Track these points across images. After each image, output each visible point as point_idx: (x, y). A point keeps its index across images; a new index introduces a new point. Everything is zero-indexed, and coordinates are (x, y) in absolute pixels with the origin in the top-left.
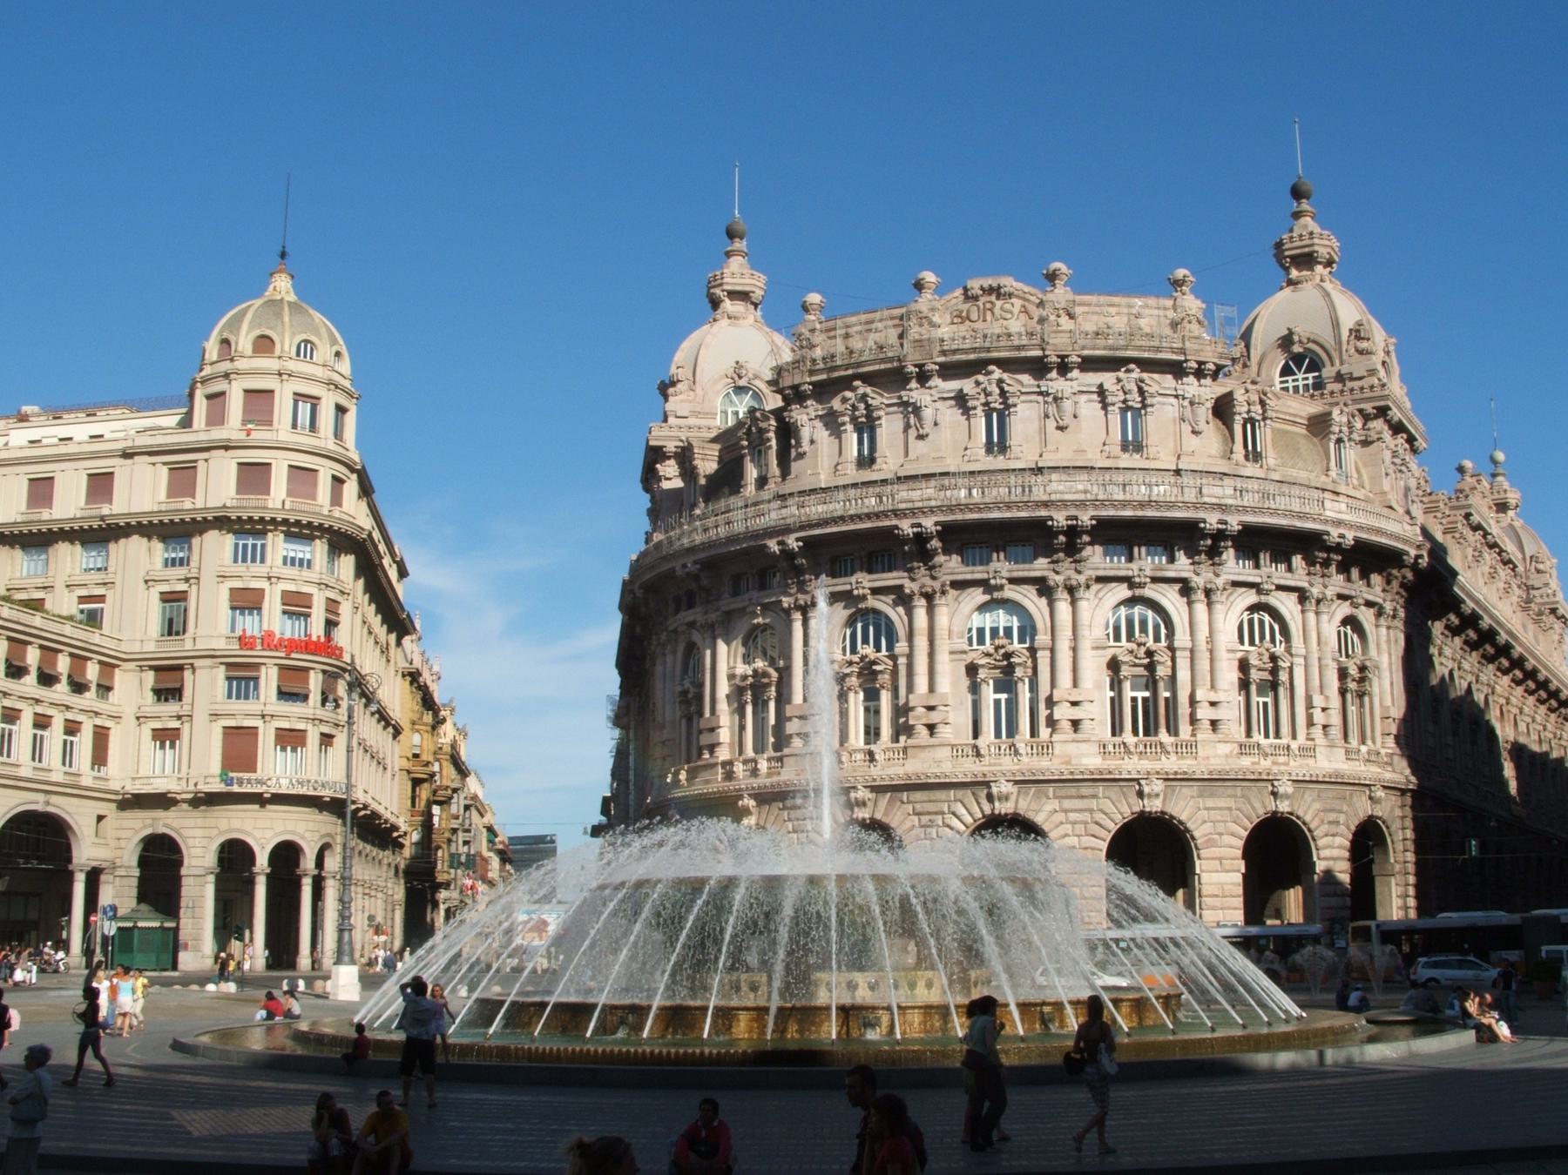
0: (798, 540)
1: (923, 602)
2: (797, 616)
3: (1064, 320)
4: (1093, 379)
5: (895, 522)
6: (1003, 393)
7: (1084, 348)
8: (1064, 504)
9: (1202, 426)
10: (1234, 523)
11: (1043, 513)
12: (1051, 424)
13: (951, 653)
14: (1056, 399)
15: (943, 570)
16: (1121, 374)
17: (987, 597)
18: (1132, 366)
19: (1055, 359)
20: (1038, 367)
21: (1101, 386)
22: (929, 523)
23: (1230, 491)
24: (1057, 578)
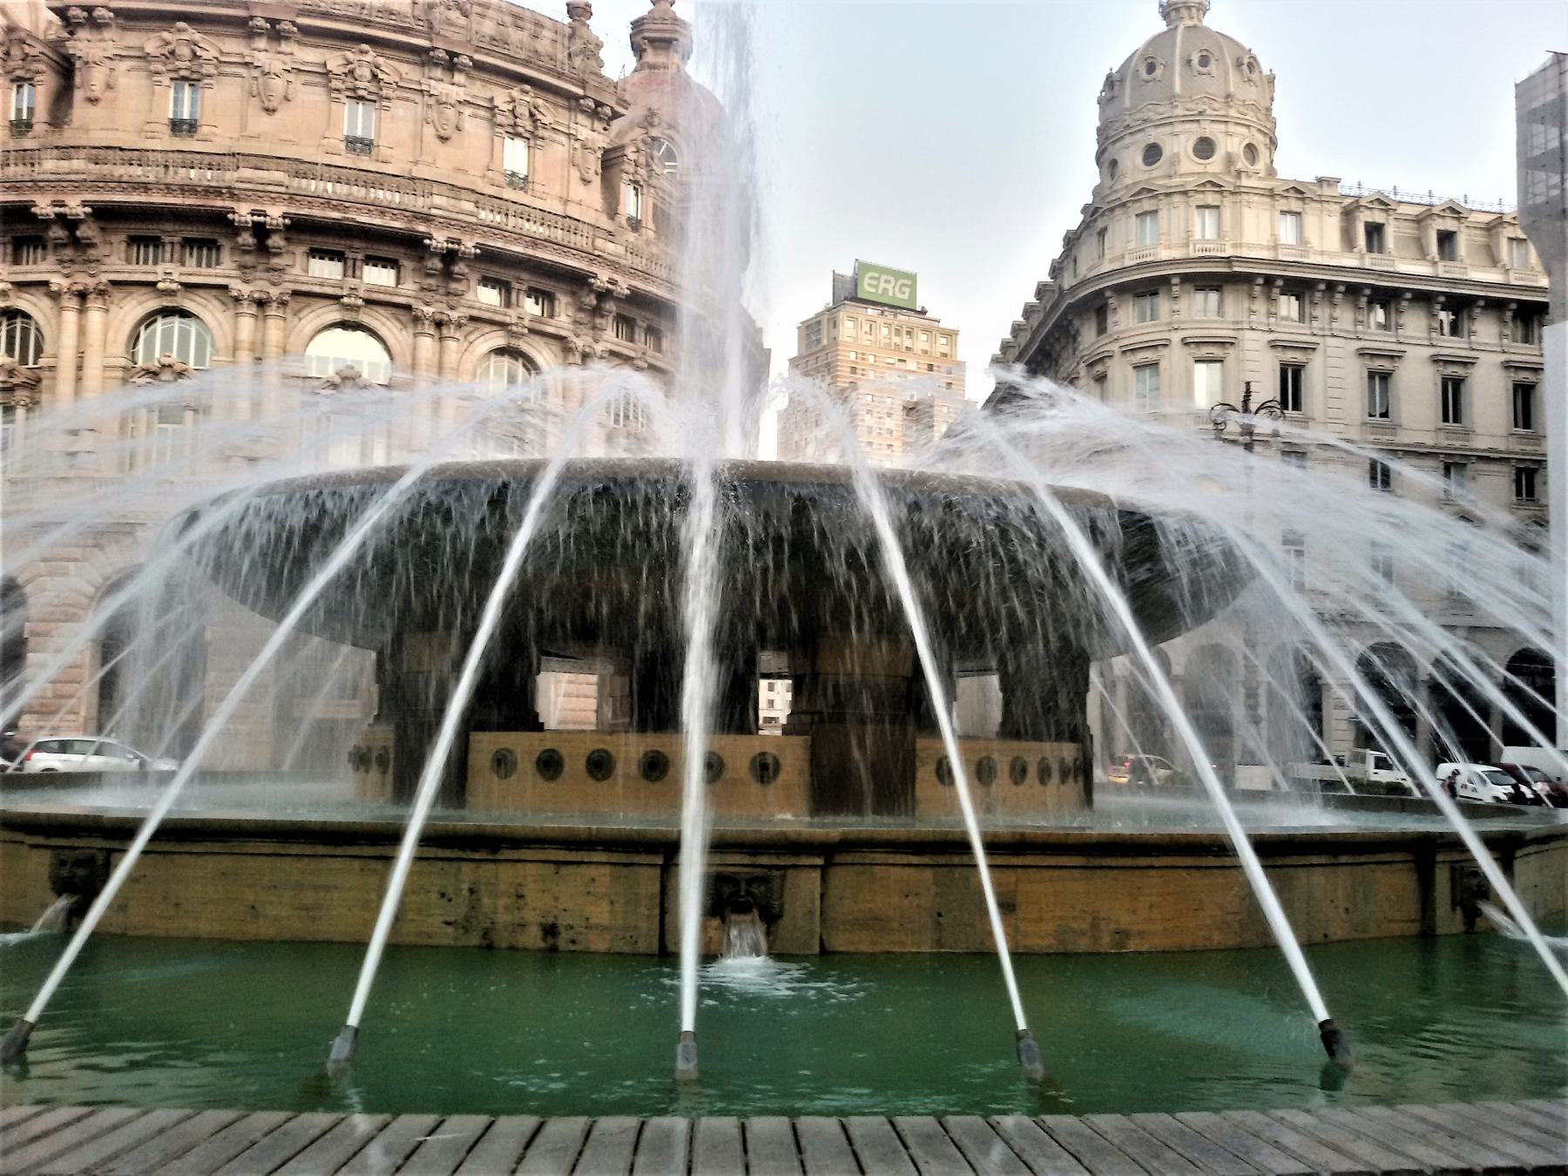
0: (85, 204)
1: (254, 310)
2: (74, 303)
3: (454, 15)
4: (479, 90)
5: (228, 204)
6: (375, 76)
7: (479, 49)
8: (448, 223)
9: (591, 175)
10: (623, 286)
11: (422, 228)
12: (429, 131)
13: (286, 377)
14: (440, 103)
15: (287, 277)
16: (515, 93)
17: (336, 316)
18: (527, 87)
19: (442, 54)
20: (423, 57)
21: (491, 100)
22: (275, 213)
23: (621, 250)
24: (426, 309)
